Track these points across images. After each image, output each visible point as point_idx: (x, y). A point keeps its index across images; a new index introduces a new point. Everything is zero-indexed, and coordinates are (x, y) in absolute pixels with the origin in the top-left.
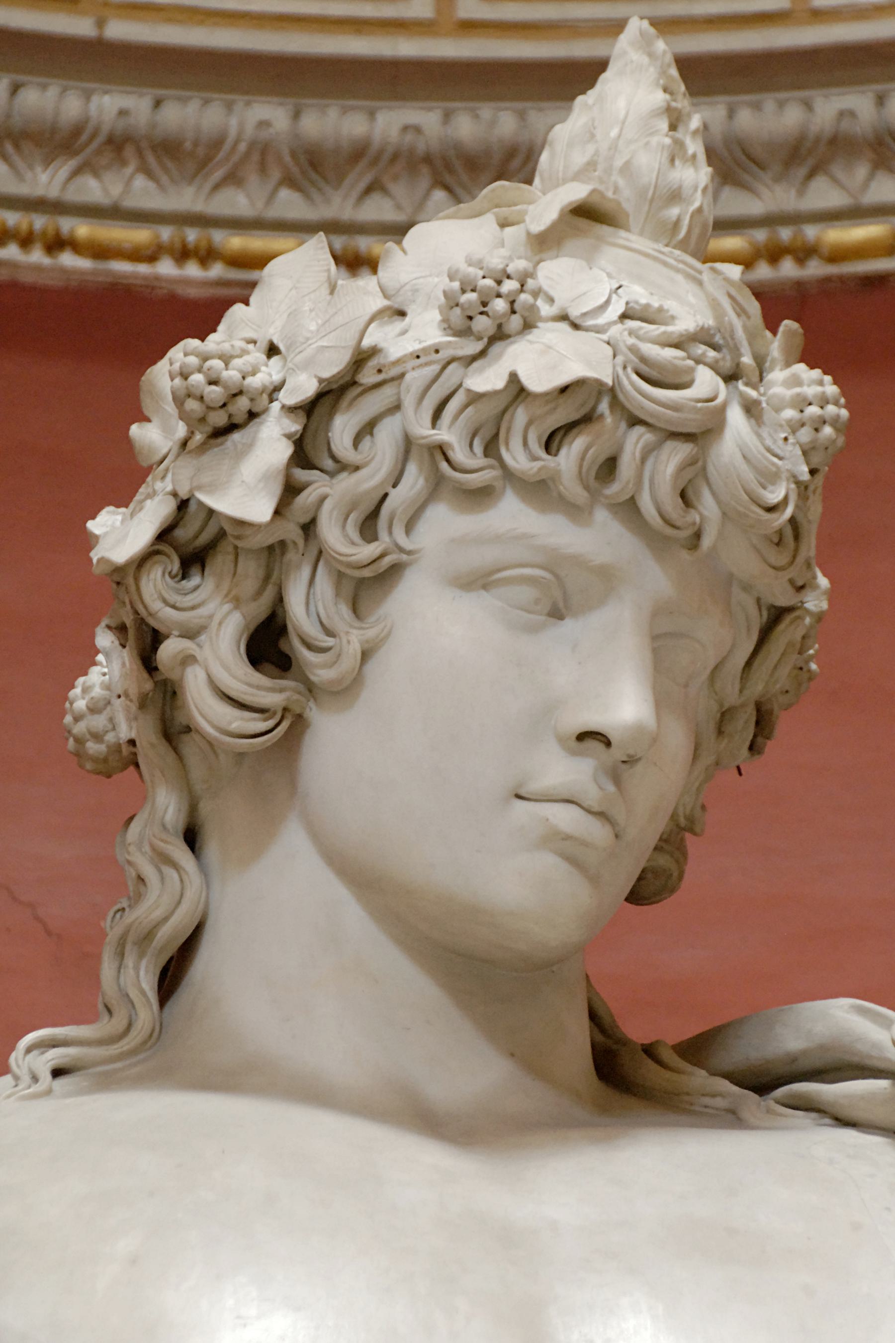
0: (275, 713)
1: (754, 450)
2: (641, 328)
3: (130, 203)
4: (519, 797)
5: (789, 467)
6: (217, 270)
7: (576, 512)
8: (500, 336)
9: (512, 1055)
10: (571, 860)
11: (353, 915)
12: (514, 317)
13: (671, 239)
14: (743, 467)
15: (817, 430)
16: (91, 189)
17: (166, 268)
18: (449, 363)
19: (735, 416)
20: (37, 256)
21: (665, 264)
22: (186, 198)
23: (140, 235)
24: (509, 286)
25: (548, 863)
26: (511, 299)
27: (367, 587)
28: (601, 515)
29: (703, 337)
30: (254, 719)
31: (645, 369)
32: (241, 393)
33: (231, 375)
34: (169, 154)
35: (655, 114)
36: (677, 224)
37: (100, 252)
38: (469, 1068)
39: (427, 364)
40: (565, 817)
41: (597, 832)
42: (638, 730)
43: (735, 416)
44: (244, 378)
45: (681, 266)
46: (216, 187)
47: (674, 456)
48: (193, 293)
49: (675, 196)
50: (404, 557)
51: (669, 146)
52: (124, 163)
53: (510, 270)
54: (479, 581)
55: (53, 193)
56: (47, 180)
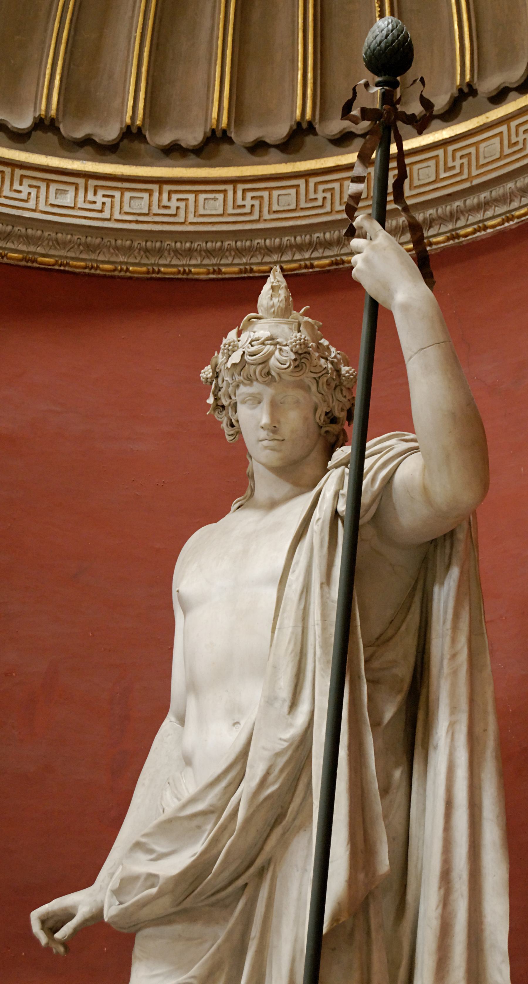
3: (496, 214)
6: (516, 221)
7: (251, 384)
8: (230, 356)
10: (272, 450)
16: (489, 214)
17: (506, 225)
19: (277, 353)
20: (483, 233)
22: (505, 209)
23: (499, 220)
24: (227, 346)
25: (268, 451)
28: (255, 383)
29: (268, 339)
33: (205, 376)
34: (498, 201)
35: (269, 290)
36: (274, 312)
37: (493, 227)
38: (286, 488)
40: (265, 443)
41: (272, 443)
42: (265, 424)
43: (277, 353)
46: (510, 204)
47: (259, 368)
48: (514, 227)
49: (273, 306)
52: (491, 206)
54: (244, 402)
55: (482, 218)
56: (479, 216)
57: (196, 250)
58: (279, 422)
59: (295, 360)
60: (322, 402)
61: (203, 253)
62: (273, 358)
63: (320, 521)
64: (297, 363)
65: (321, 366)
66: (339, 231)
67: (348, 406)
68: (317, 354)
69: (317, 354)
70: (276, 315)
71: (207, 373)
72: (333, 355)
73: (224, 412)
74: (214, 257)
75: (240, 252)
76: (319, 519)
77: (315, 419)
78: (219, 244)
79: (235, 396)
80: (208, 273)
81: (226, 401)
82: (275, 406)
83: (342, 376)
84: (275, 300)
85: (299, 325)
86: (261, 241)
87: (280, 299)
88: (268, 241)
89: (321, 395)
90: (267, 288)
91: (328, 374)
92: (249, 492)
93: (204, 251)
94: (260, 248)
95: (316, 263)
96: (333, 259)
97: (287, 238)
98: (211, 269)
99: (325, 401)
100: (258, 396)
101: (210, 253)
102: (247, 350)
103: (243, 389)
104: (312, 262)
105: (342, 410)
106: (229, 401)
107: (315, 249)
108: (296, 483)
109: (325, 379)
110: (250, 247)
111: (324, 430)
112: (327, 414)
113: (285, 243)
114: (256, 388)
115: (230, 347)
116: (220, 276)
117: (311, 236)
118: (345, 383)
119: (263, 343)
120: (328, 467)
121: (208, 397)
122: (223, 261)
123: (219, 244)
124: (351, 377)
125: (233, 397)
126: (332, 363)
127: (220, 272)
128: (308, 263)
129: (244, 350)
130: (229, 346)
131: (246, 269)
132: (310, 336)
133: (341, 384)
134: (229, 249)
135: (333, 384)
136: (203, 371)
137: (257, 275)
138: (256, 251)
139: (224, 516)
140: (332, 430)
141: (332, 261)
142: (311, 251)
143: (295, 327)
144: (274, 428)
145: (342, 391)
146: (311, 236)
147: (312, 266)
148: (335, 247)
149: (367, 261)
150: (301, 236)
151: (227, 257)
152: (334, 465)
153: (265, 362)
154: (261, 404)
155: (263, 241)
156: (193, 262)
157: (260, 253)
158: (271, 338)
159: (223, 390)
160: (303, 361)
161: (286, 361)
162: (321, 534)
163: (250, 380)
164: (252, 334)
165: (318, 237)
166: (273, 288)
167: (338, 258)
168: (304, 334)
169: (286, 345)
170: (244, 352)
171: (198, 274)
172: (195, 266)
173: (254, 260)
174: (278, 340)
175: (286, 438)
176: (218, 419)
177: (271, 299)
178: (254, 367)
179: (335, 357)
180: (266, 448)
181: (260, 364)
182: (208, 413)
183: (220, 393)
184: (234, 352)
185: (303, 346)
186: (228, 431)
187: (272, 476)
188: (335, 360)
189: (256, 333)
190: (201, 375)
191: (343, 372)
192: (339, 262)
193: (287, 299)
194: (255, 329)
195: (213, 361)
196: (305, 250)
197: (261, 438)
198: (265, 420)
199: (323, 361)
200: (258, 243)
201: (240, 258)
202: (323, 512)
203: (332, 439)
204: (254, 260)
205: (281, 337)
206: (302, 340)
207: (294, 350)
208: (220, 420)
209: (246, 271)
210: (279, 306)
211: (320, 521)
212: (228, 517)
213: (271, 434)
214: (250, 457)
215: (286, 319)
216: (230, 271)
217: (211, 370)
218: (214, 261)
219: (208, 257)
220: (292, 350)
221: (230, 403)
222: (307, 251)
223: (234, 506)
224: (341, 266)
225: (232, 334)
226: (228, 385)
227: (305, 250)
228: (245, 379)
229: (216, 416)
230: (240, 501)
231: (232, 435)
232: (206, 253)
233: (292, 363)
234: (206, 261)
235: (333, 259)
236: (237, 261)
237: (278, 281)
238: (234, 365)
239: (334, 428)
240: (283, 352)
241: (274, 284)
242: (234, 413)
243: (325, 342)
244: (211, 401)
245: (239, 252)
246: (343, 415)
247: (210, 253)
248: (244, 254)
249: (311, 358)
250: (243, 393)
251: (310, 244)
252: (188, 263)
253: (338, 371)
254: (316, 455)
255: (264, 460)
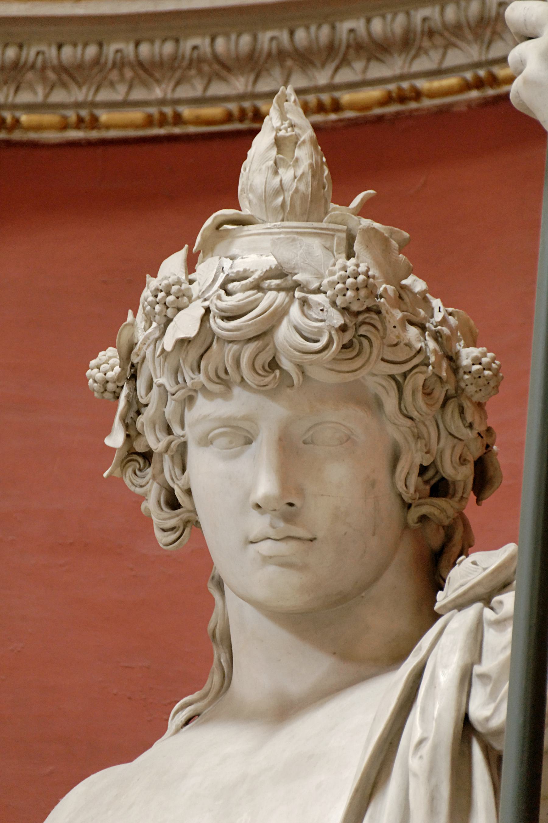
0: (179, 527)
1: (303, 325)
2: (234, 286)
4: (252, 542)
5: (327, 323)
7: (226, 394)
8: (169, 321)
9: (335, 653)
10: (282, 565)
11: (248, 609)
12: (169, 310)
13: (284, 214)
14: (286, 343)
15: (345, 295)
18: (156, 341)
19: (295, 310)
21: (271, 234)
24: (161, 295)
25: (271, 570)
26: (163, 302)
27: (181, 455)
28: (237, 390)
29: (270, 275)
30: (170, 535)
31: (223, 314)
32: (107, 382)
33: (99, 376)
35: (269, 149)
39: (149, 345)
40: (266, 547)
41: (284, 548)
42: (266, 498)
43: (295, 310)
44: (105, 374)
45: (281, 230)
47: (248, 351)
49: (281, 189)
50: (183, 439)
51: (271, 166)
53: (160, 287)
54: (206, 441)
57: (33, 67)
58: (301, 491)
59: (343, 329)
60: (411, 439)
61: (52, 75)
62: (285, 322)
63: (426, 748)
64: (348, 336)
65: (408, 345)
66: (408, 13)
67: (475, 451)
68: (398, 315)
69: (398, 315)
70: (286, 212)
71: (104, 367)
72: (438, 317)
73: (149, 471)
74: (80, 86)
75: (147, 71)
76: (421, 742)
77: (394, 485)
78: (92, 51)
79: (183, 427)
80: (65, 126)
81: (159, 441)
82: (291, 452)
83: (461, 371)
84: (286, 175)
85: (351, 239)
86: (202, 42)
87: (299, 173)
88: (220, 42)
89: (409, 422)
90: (262, 144)
91: (427, 365)
92: (215, 678)
93: (54, 69)
94: (201, 60)
95: (346, 97)
96: (392, 87)
97: (269, 34)
98: (72, 115)
99: (418, 437)
100: (245, 425)
101: (69, 74)
102: (215, 305)
103: (203, 407)
104: (337, 94)
105: (463, 461)
106: (165, 439)
107: (345, 62)
108: (345, 653)
109: (421, 379)
110: (174, 57)
111: (414, 514)
112: (423, 470)
113: (266, 46)
114: (238, 404)
115: (171, 298)
116: (94, 134)
117: (333, 28)
118: (471, 389)
119: (257, 287)
120: (437, 607)
121: (108, 431)
122: (104, 95)
123: (92, 51)
124: (487, 373)
125: (176, 429)
126: (437, 336)
127: (94, 123)
128: (326, 98)
129: (207, 304)
130: (168, 294)
131: (163, 115)
132: (379, 265)
133: (459, 391)
134: (120, 64)
135: (439, 394)
136: (93, 363)
137: (192, 129)
138: (190, 66)
139: (149, 745)
140: (436, 512)
141: (389, 93)
142: (333, 65)
143: (338, 244)
144: (288, 509)
145: (462, 412)
146: (333, 28)
147: (337, 107)
148: (396, 55)
149: (547, 56)
150: (307, 28)
151: (112, 84)
152: (454, 600)
153: (264, 334)
154: (254, 444)
155: (207, 41)
156: (25, 97)
157: (200, 72)
158: (279, 273)
159: (148, 413)
160: (363, 330)
161: (320, 332)
162: (429, 779)
163: (224, 381)
164: (227, 263)
165: (352, 31)
166: (278, 143)
167: (405, 85)
168: (364, 262)
169: (318, 291)
170: (208, 310)
171: (39, 128)
172: (30, 108)
173: (184, 92)
174: (295, 278)
175: (320, 535)
176: (132, 488)
177: (276, 173)
178: (235, 347)
179: (444, 322)
180: (267, 560)
181: (250, 340)
182: (105, 475)
183: (141, 420)
184: (179, 310)
185: (363, 293)
186: (160, 517)
187: (280, 636)
188: (446, 330)
189: (238, 261)
190: (89, 372)
191: (465, 361)
192: (408, 94)
193: (315, 171)
194: (234, 251)
195: (123, 336)
196: (318, 64)
197: (252, 538)
198: (265, 486)
199: (413, 332)
200: (195, 48)
201: (145, 85)
202: (431, 724)
203: (435, 540)
204: (184, 92)
205: (304, 270)
206: (361, 278)
207: (338, 302)
208: (138, 490)
209: (163, 121)
210: (297, 190)
211: (426, 748)
212: (159, 746)
213: (281, 524)
214: (220, 585)
215: (316, 224)
216: (119, 122)
217: (117, 360)
218: (79, 95)
219: (64, 85)
220: (334, 304)
221: (170, 443)
222: (323, 65)
223: (176, 720)
224: (413, 105)
225: (173, 266)
226: (165, 393)
227: (318, 64)
228: (210, 379)
229: (127, 482)
230: (190, 704)
231: (172, 529)
232: (58, 75)
233: (335, 337)
234: (59, 96)
235: (392, 87)
236: (138, 94)
237: (292, 126)
238: (183, 343)
239: (440, 509)
240: (310, 307)
241: (282, 133)
242: (178, 471)
243: (418, 285)
244: (116, 439)
245: (146, 70)
246: (463, 475)
247: (69, 74)
248: (157, 75)
249: (383, 322)
250: (205, 417)
251: (331, 49)
252: (10, 99)
253: (452, 359)
254: (398, 581)
255: (260, 592)
